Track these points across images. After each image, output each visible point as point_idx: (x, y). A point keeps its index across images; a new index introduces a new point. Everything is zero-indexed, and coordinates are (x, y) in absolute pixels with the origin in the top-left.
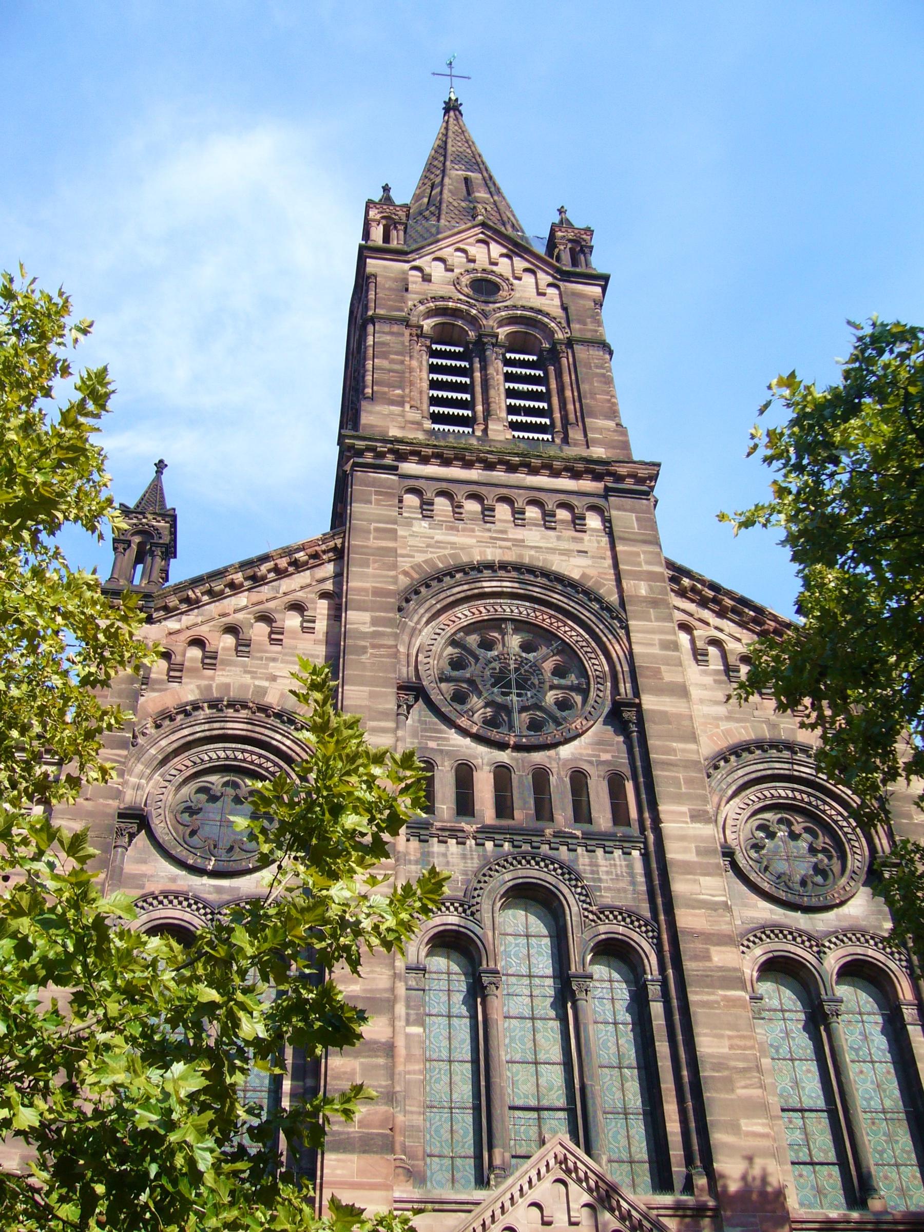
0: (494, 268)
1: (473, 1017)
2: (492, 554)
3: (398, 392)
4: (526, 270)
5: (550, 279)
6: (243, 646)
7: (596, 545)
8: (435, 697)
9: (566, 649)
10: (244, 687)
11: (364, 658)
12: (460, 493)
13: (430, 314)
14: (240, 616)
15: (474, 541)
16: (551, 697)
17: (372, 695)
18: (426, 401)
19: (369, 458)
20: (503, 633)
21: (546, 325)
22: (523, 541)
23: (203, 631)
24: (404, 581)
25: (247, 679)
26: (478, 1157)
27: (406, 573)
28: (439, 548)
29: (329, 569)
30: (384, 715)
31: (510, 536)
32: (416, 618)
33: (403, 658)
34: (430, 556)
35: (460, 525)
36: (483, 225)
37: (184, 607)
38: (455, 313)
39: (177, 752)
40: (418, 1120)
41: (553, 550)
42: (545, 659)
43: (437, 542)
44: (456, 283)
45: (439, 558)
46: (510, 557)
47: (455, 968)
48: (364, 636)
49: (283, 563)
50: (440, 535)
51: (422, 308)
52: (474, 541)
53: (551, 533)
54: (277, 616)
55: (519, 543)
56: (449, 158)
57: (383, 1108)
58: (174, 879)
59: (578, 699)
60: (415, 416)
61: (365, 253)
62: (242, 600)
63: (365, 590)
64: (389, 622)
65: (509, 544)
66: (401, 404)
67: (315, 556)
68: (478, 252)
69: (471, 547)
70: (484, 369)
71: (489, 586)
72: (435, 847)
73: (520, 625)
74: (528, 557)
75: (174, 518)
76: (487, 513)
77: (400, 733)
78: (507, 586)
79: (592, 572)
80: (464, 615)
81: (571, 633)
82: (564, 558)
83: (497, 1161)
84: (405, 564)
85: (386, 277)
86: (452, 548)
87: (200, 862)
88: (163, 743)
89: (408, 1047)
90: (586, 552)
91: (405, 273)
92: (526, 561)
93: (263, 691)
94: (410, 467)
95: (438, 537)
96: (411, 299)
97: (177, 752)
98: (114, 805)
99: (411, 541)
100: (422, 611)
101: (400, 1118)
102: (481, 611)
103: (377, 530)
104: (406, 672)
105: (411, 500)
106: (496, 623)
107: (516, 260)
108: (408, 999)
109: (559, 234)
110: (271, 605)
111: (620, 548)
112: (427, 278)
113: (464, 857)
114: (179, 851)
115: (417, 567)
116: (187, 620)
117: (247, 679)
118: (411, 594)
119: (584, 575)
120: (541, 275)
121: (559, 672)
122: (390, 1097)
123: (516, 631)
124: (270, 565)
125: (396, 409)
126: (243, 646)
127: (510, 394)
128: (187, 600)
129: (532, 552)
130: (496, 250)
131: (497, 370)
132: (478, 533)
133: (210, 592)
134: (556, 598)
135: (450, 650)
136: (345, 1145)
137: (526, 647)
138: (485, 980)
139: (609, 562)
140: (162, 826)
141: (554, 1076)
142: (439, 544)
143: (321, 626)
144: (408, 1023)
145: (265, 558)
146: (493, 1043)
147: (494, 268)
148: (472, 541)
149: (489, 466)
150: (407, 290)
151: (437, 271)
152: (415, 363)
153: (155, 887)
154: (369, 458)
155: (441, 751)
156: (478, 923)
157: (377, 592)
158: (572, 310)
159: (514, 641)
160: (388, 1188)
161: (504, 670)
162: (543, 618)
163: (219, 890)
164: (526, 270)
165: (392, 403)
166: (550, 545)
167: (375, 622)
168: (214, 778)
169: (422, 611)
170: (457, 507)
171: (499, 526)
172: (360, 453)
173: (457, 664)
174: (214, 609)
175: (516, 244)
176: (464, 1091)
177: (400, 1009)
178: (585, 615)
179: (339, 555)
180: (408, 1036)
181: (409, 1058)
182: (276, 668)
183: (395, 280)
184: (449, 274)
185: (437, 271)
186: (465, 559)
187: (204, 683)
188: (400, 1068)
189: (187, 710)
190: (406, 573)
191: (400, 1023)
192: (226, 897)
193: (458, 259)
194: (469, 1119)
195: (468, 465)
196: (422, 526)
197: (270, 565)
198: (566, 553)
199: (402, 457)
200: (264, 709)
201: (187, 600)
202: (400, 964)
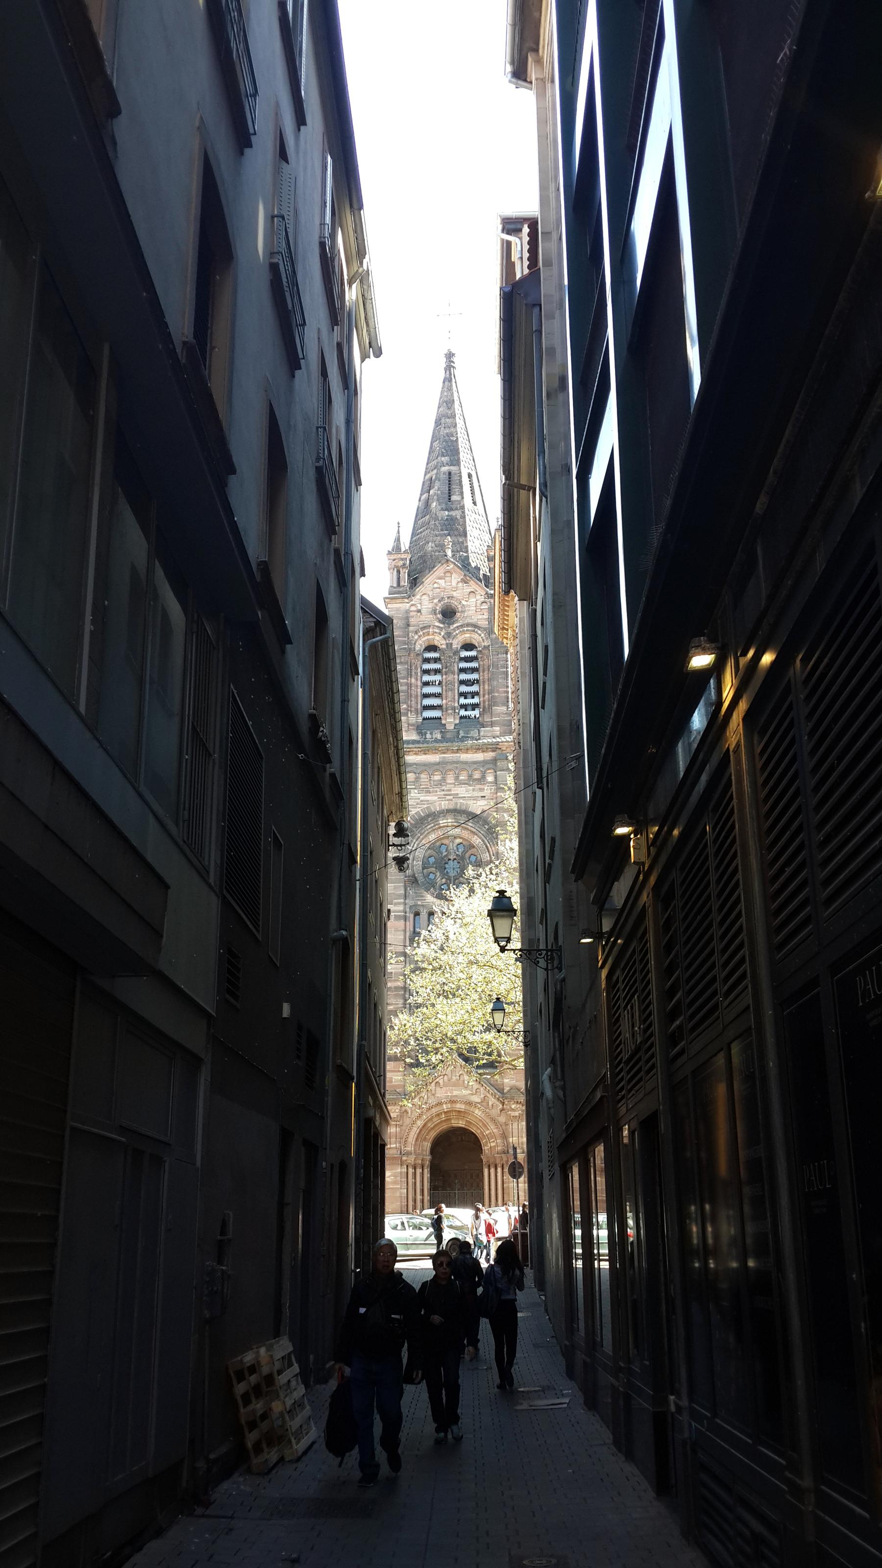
0: (455, 594)
2: (445, 805)
7: (489, 791)
15: (437, 798)
22: (458, 794)
28: (422, 804)
31: (453, 792)
32: (412, 845)
34: (418, 809)
43: (421, 801)
51: (416, 637)
52: (437, 798)
55: (456, 796)
65: (451, 797)
69: (435, 802)
77: (407, 901)
82: (475, 802)
85: (399, 618)
86: (427, 804)
90: (485, 797)
92: (458, 807)
95: (422, 798)
100: (415, 841)
120: (478, 597)
132: (439, 793)
150: (409, 625)
155: (423, 905)
166: (469, 795)
169: (415, 841)
198: (475, 798)
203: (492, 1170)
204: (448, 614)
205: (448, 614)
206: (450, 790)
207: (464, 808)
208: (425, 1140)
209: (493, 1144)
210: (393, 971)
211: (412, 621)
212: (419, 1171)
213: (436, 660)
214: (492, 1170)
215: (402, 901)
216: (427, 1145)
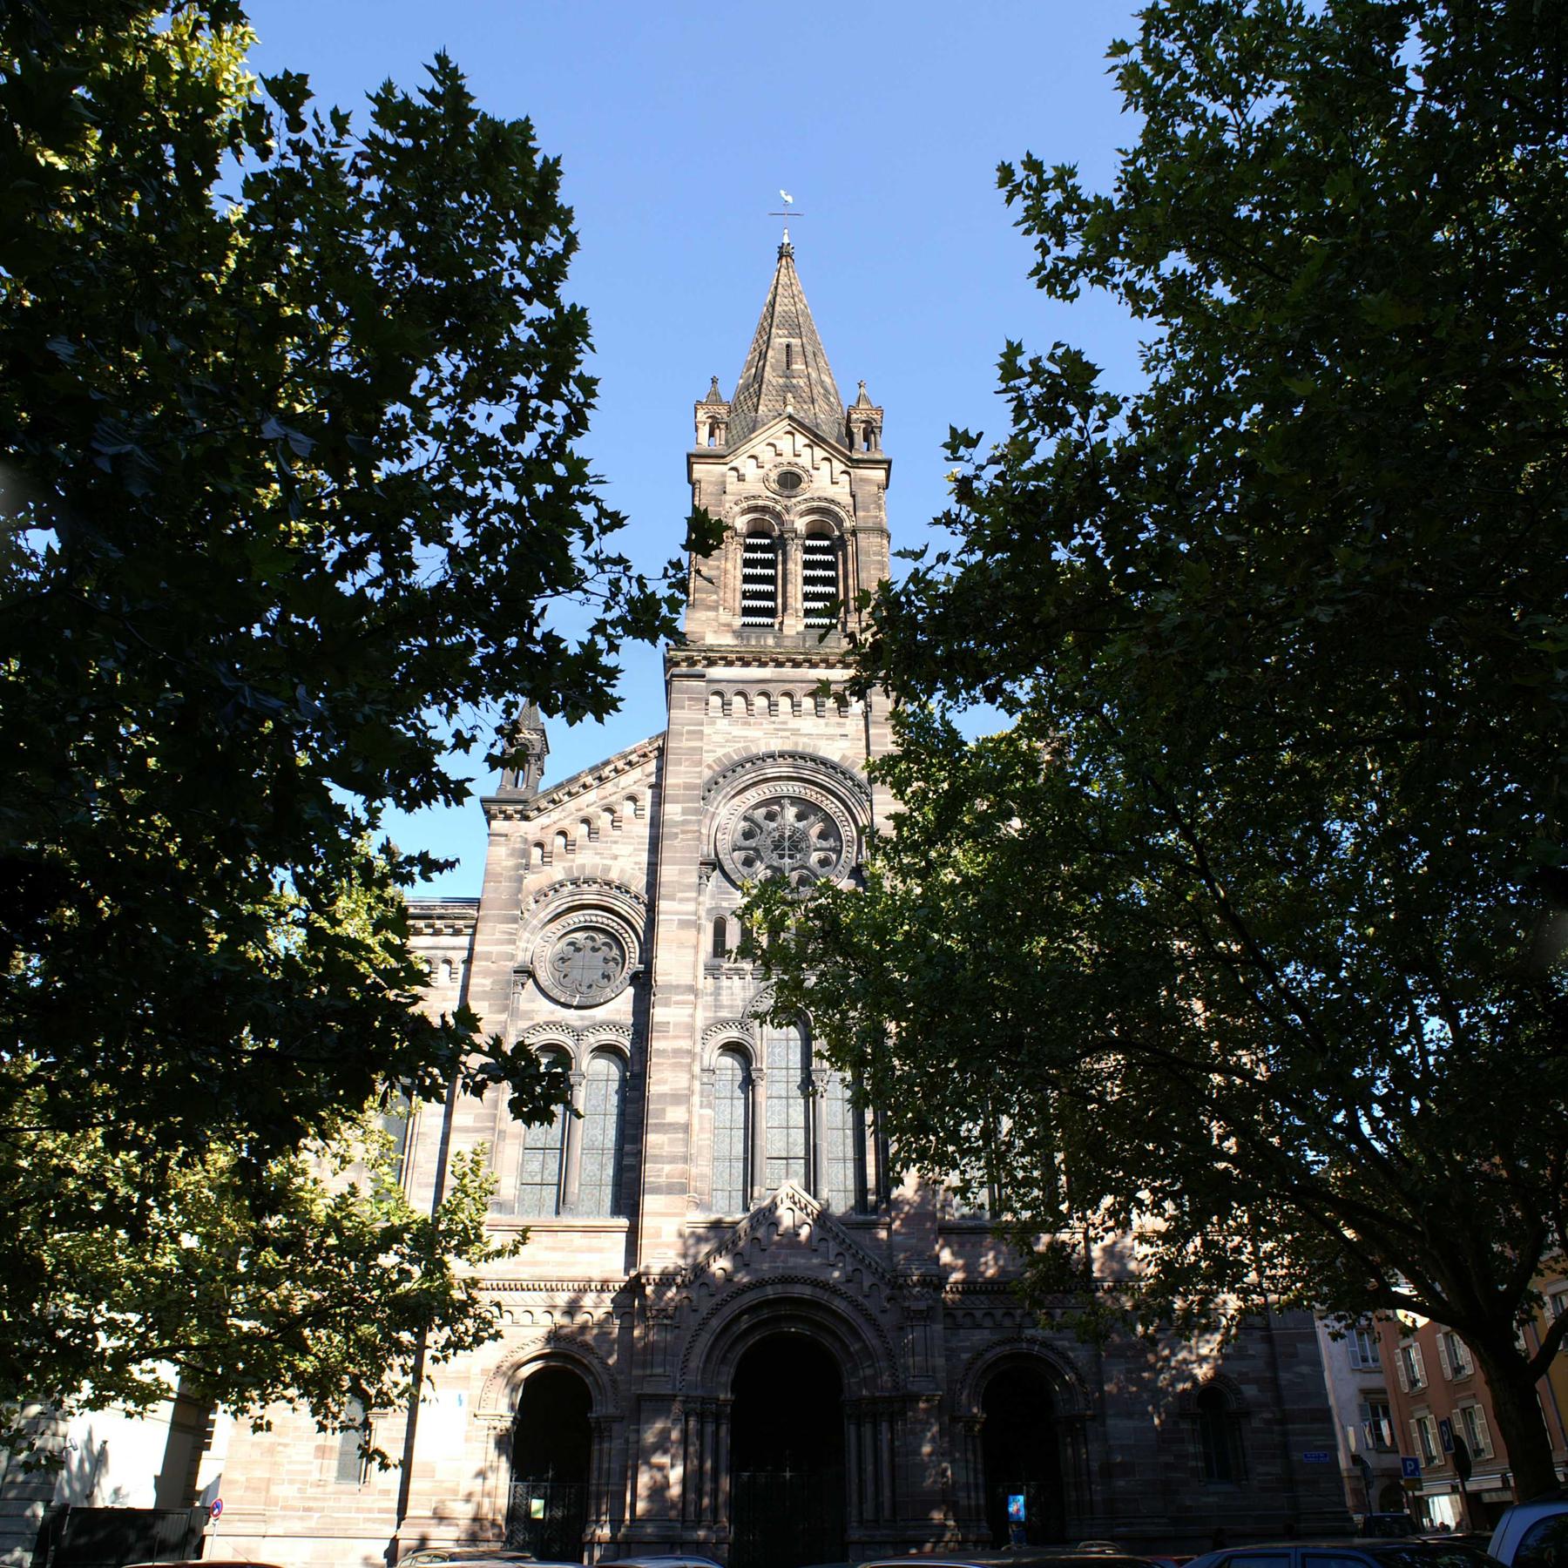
1: (747, 1099)
2: (776, 745)
3: (714, 597)
4: (825, 459)
5: (843, 467)
6: (593, 833)
8: (728, 867)
9: (827, 818)
10: (595, 866)
11: (676, 843)
12: (752, 691)
13: (744, 512)
14: (591, 810)
16: (815, 857)
17: (681, 872)
18: (739, 596)
19: (684, 668)
20: (782, 808)
21: (837, 514)
23: (565, 824)
24: (707, 774)
25: (597, 860)
26: (745, 1190)
27: (709, 767)
29: (652, 766)
30: (688, 887)
31: (790, 726)
33: (705, 839)
35: (752, 720)
36: (790, 417)
37: (551, 806)
38: (764, 509)
39: (551, 920)
40: (707, 1170)
41: (820, 736)
42: (812, 825)
44: (765, 480)
45: (734, 751)
46: (788, 746)
47: (737, 1065)
48: (676, 824)
49: (620, 765)
50: (738, 731)
53: (821, 721)
54: (617, 808)
55: (796, 732)
56: (776, 321)
57: (681, 1166)
58: (552, 1013)
59: (834, 857)
60: (724, 617)
61: (691, 459)
62: (591, 796)
63: (678, 786)
64: (697, 812)
66: (715, 609)
67: (645, 755)
68: (785, 444)
70: (785, 562)
71: (771, 772)
72: (725, 982)
73: (795, 800)
74: (804, 745)
75: (543, 731)
76: (772, 706)
78: (785, 771)
79: (850, 753)
80: (753, 796)
81: (831, 806)
83: (756, 1194)
84: (709, 758)
87: (569, 1000)
88: (542, 915)
89: (701, 1123)
91: (724, 475)
92: (800, 749)
93: (607, 869)
94: (717, 672)
95: (735, 733)
96: (729, 499)
97: (551, 920)
98: (512, 965)
99: (716, 738)
101: (694, 1171)
102: (765, 791)
103: (689, 732)
104: (707, 850)
105: (715, 701)
106: (777, 800)
107: (816, 449)
108: (702, 1092)
109: (854, 416)
110: (613, 798)
111: (871, 731)
112: (741, 478)
113: (744, 988)
114: (555, 993)
115: (718, 761)
116: (555, 815)
117: (597, 860)
118: (712, 785)
119: (844, 757)
121: (823, 836)
122: (686, 1159)
123: (792, 804)
124: (611, 767)
125: (711, 614)
126: (593, 833)
127: (808, 581)
128: (553, 801)
129: (805, 740)
130: (801, 440)
131: (797, 557)
133: (569, 794)
134: (821, 778)
135: (743, 824)
136: (657, 1190)
137: (800, 817)
138: (754, 1075)
139: (864, 742)
140: (543, 976)
141: (799, 1136)
142: (735, 739)
143: (647, 813)
144: (701, 1106)
145: (607, 763)
146: (758, 1119)
147: (797, 460)
148: (759, 734)
149: (779, 664)
151: (748, 468)
152: (730, 566)
153: (540, 1019)
154: (684, 668)
156: (752, 1036)
157: (688, 787)
158: (859, 499)
159: (791, 812)
160: (683, 1215)
161: (782, 837)
162: (811, 794)
163: (582, 1018)
164: (825, 459)
165: (710, 608)
167: (685, 812)
168: (579, 935)
170: (749, 703)
171: (782, 718)
172: (677, 664)
173: (748, 835)
174: (572, 805)
175: (816, 435)
176: (739, 1148)
177: (696, 1099)
178: (842, 791)
179: (661, 752)
180: (701, 1116)
181: (702, 1129)
182: (616, 849)
183: (716, 484)
184: (761, 471)
185: (748, 468)
186: (755, 751)
187: (567, 865)
188: (695, 1138)
189: (556, 888)
190: (709, 767)
191: (696, 1109)
192: (587, 1023)
193: (767, 455)
194: (741, 1165)
195: (763, 664)
196: (722, 724)
197: (611, 767)
198: (831, 737)
199: (711, 663)
200: (608, 884)
201: (553, 801)
202: (697, 1069)
203: (867, 1430)
204: (790, 481)
205: (790, 481)
206: (784, 723)
207: (809, 750)
208: (724, 1360)
209: (869, 1372)
210: (671, 1020)
211: (729, 488)
212: (710, 1428)
213: (764, 549)
214: (867, 1430)
215: (694, 895)
216: (727, 1374)
